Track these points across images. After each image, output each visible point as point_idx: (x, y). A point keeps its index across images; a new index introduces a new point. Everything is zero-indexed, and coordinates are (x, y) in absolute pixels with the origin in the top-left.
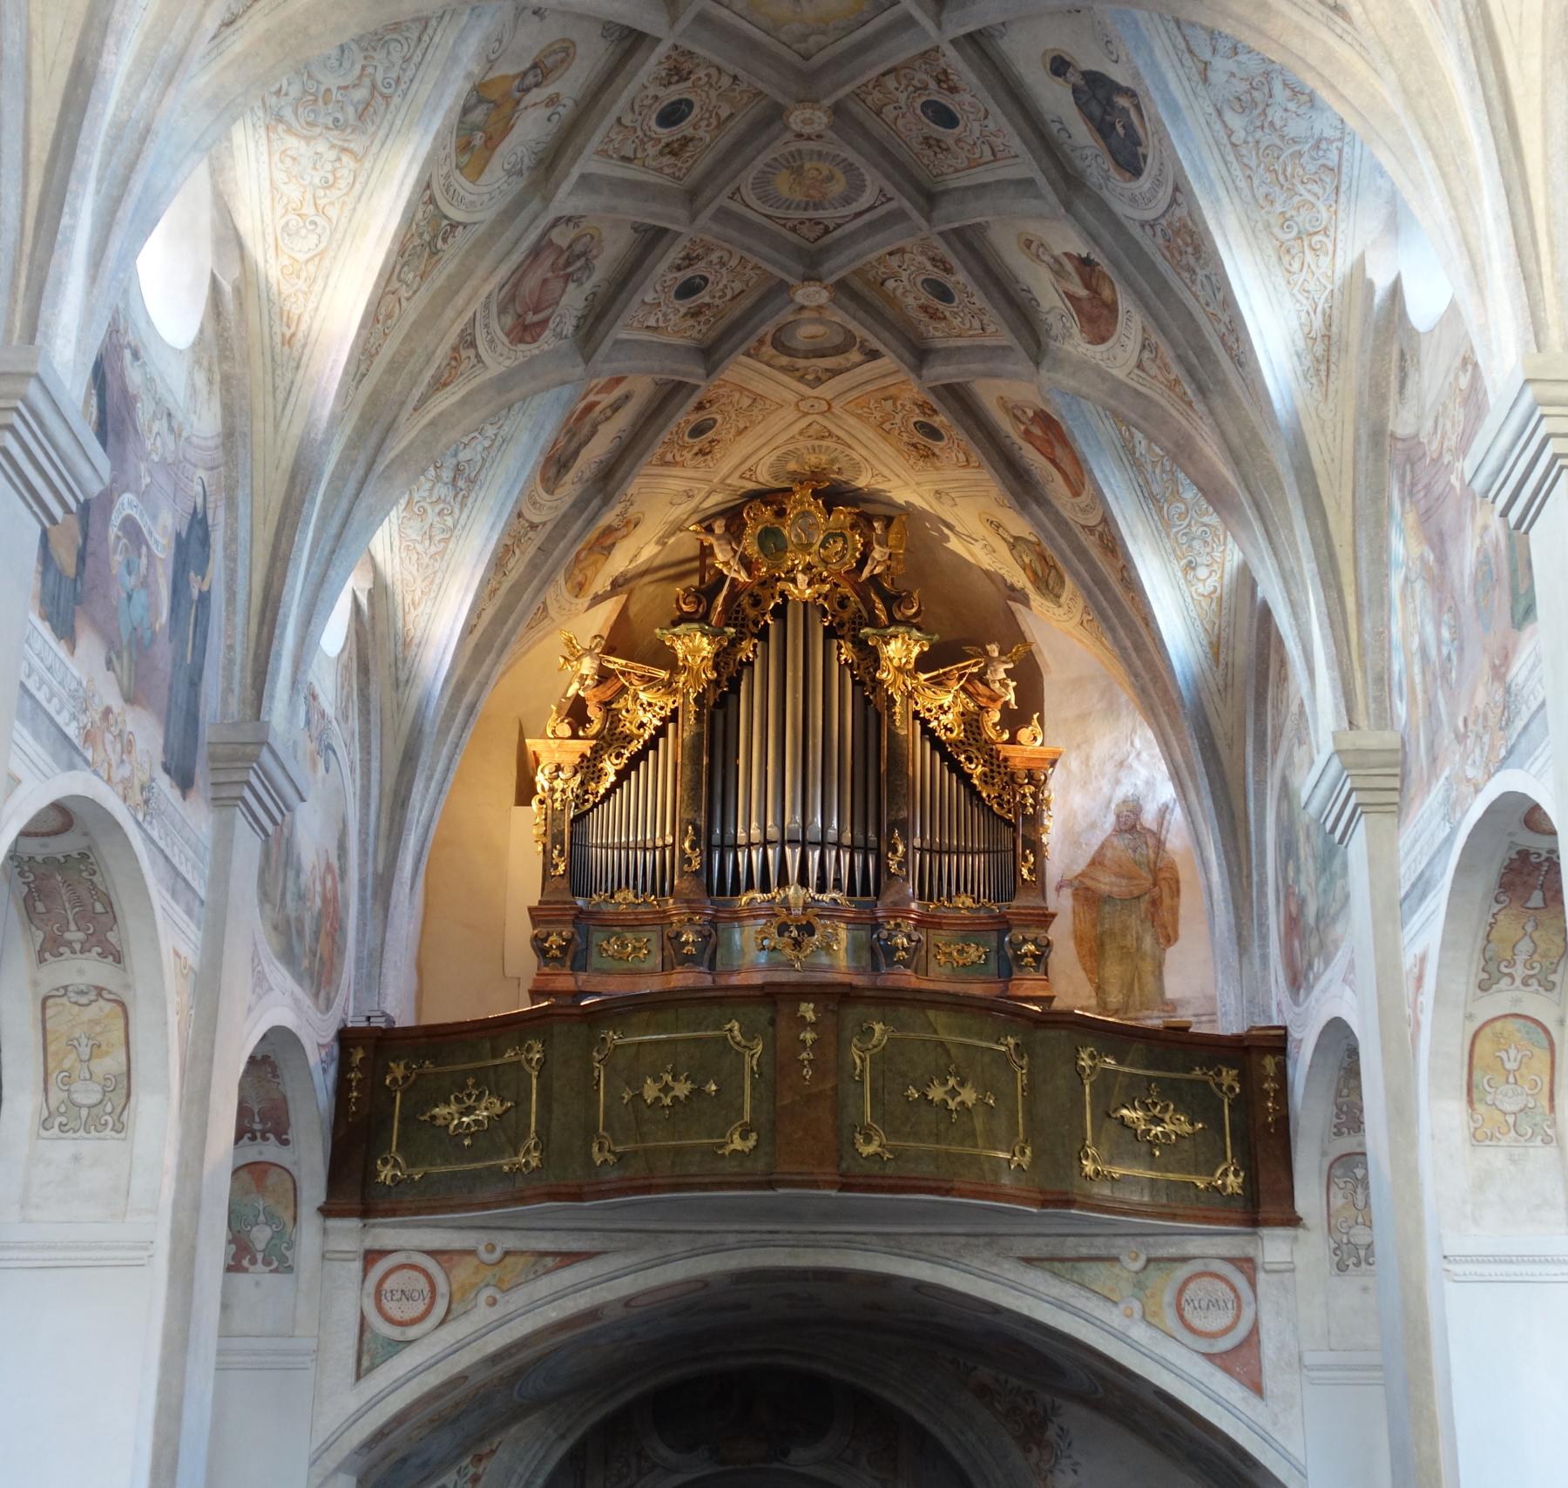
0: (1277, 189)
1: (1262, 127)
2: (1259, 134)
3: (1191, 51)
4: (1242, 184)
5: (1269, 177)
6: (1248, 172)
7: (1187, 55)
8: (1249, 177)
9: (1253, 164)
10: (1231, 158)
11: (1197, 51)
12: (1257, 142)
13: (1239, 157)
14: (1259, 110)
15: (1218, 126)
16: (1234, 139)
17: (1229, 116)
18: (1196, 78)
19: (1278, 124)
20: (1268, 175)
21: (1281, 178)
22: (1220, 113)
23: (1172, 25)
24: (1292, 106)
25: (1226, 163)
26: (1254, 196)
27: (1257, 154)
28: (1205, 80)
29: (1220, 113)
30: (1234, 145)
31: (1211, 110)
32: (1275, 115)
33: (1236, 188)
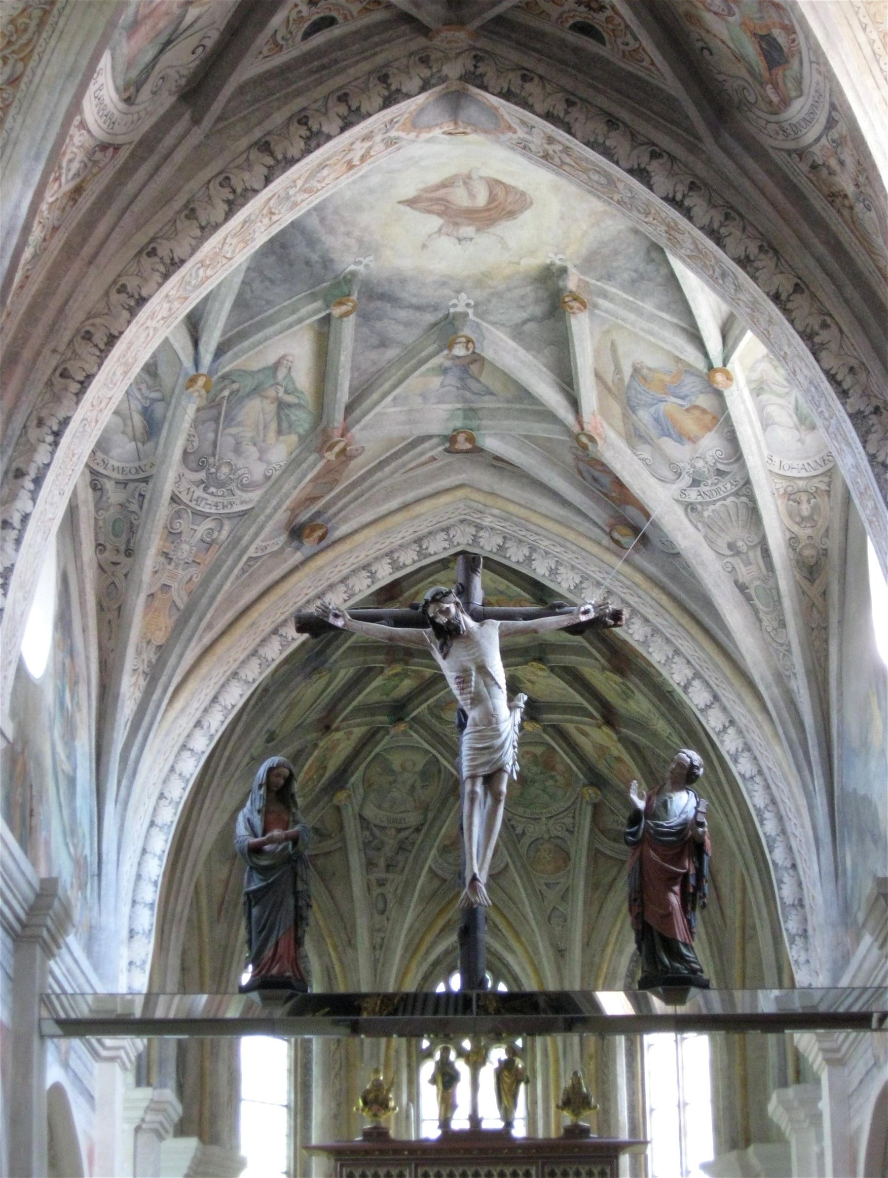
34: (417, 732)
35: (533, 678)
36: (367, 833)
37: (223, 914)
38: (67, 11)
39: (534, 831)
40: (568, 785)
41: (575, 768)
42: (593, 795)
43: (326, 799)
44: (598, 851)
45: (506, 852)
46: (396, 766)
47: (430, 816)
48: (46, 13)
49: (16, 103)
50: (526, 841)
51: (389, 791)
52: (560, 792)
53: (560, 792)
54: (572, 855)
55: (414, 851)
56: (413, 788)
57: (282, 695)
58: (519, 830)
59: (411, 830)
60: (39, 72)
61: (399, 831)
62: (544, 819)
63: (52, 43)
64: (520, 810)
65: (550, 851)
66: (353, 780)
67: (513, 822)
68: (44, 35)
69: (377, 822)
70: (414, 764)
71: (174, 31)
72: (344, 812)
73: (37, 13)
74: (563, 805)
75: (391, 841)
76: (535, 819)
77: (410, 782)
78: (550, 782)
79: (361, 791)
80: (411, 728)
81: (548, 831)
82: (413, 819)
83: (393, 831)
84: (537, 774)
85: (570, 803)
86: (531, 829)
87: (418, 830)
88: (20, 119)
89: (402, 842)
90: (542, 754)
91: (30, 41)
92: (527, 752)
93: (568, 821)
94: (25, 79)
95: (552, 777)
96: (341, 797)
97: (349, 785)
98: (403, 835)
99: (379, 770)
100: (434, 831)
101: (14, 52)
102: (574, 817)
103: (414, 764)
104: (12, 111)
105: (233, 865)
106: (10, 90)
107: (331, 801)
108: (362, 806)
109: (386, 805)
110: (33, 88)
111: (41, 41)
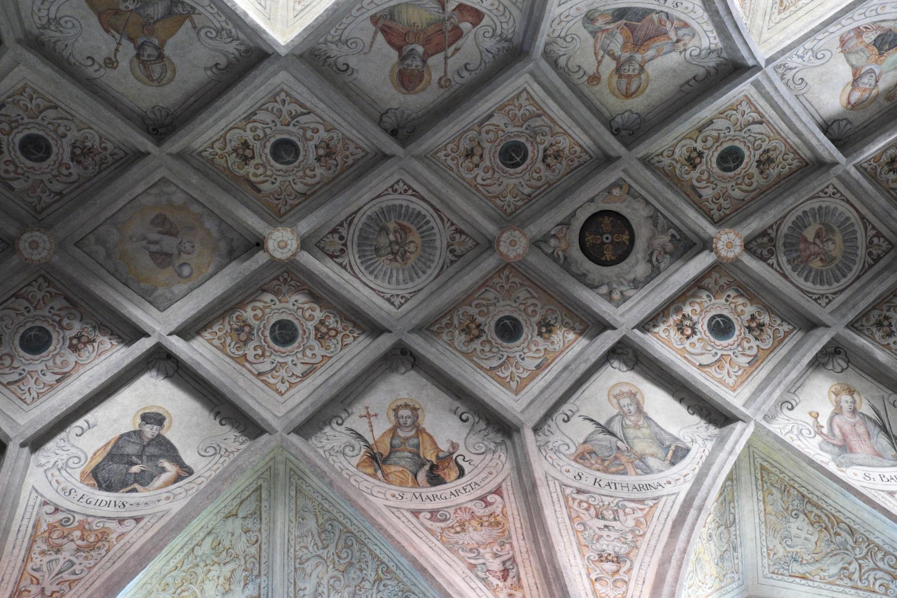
0: (173, 590)
1: (206, 565)
2: (202, 564)
3: (241, 503)
4: (172, 564)
5: (178, 582)
6: (179, 566)
7: (238, 500)
8: (177, 567)
9: (185, 568)
10: (186, 550)
11: (242, 506)
12: (197, 565)
13: (187, 556)
14: (216, 559)
15: (202, 535)
16: (197, 548)
17: (209, 539)
18: (227, 511)
19: (210, 575)
20: (180, 580)
21: (179, 591)
22: (209, 533)
23: (255, 486)
24: (222, 580)
25: (182, 548)
26: (165, 576)
27: (191, 568)
28: (227, 517)
29: (209, 533)
30: (193, 549)
31: (210, 527)
32: (215, 571)
33: (168, 561)
38: (810, 488)
48: (809, 502)
49: (867, 534)
60: (848, 514)
63: (830, 502)
68: (824, 505)
71: (875, 422)
73: (809, 507)
88: (877, 534)
91: (827, 515)
94: (852, 524)
101: (832, 528)
104: (871, 537)
106: (857, 536)
110: (858, 521)
111: (828, 508)
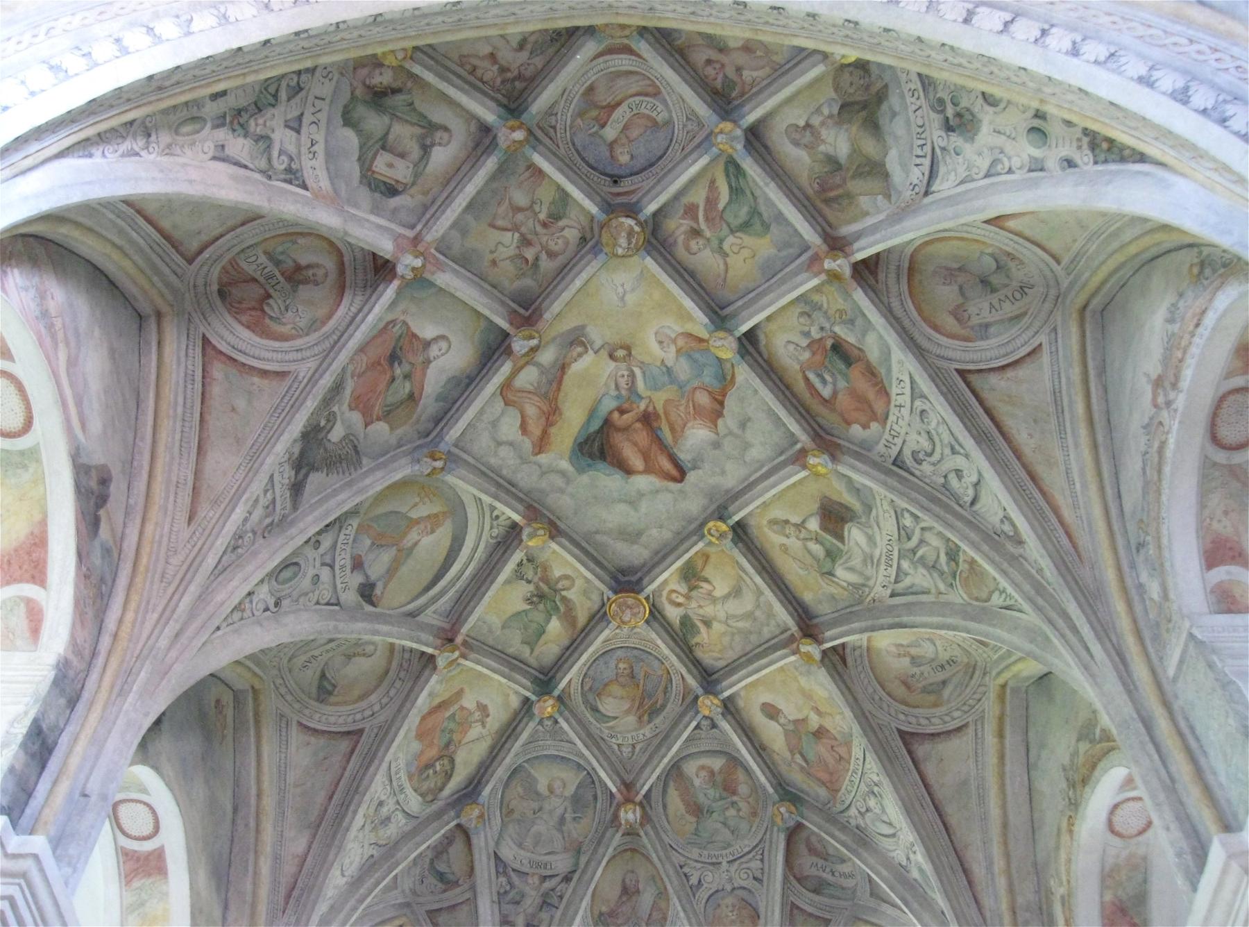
34: (567, 720)
35: (709, 610)
36: (503, 880)
37: (292, 901)
39: (712, 880)
40: (754, 814)
41: (763, 779)
42: (786, 815)
43: (452, 813)
44: (794, 906)
45: (677, 904)
46: (542, 787)
47: (583, 859)
50: (703, 894)
51: (534, 823)
52: (744, 826)
53: (744, 826)
54: (762, 910)
55: (562, 907)
56: (562, 820)
57: (379, 474)
58: (694, 880)
59: (558, 879)
61: (544, 878)
62: (724, 864)
64: (694, 853)
65: (734, 906)
66: (486, 791)
67: (686, 870)
69: (517, 866)
70: (564, 785)
72: (475, 841)
74: (747, 843)
75: (533, 893)
76: (713, 864)
77: (559, 811)
78: (732, 812)
79: (496, 822)
80: (561, 714)
81: (730, 880)
82: (561, 864)
83: (536, 880)
84: (715, 800)
85: (759, 838)
86: (709, 879)
87: (567, 879)
89: (546, 895)
90: (721, 769)
92: (703, 767)
93: (756, 864)
95: (733, 804)
96: (471, 815)
97: (481, 800)
98: (548, 885)
99: (520, 790)
100: (587, 877)
102: (762, 860)
103: (564, 785)
105: (314, 836)
107: (458, 816)
108: (497, 843)
109: (529, 842)
